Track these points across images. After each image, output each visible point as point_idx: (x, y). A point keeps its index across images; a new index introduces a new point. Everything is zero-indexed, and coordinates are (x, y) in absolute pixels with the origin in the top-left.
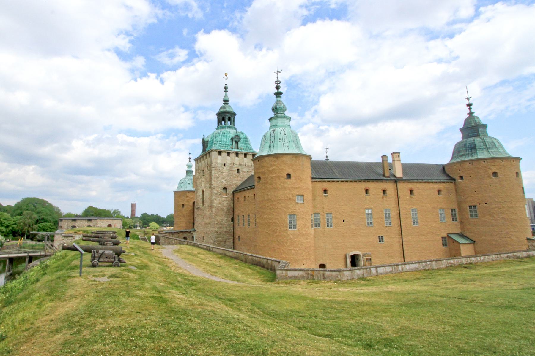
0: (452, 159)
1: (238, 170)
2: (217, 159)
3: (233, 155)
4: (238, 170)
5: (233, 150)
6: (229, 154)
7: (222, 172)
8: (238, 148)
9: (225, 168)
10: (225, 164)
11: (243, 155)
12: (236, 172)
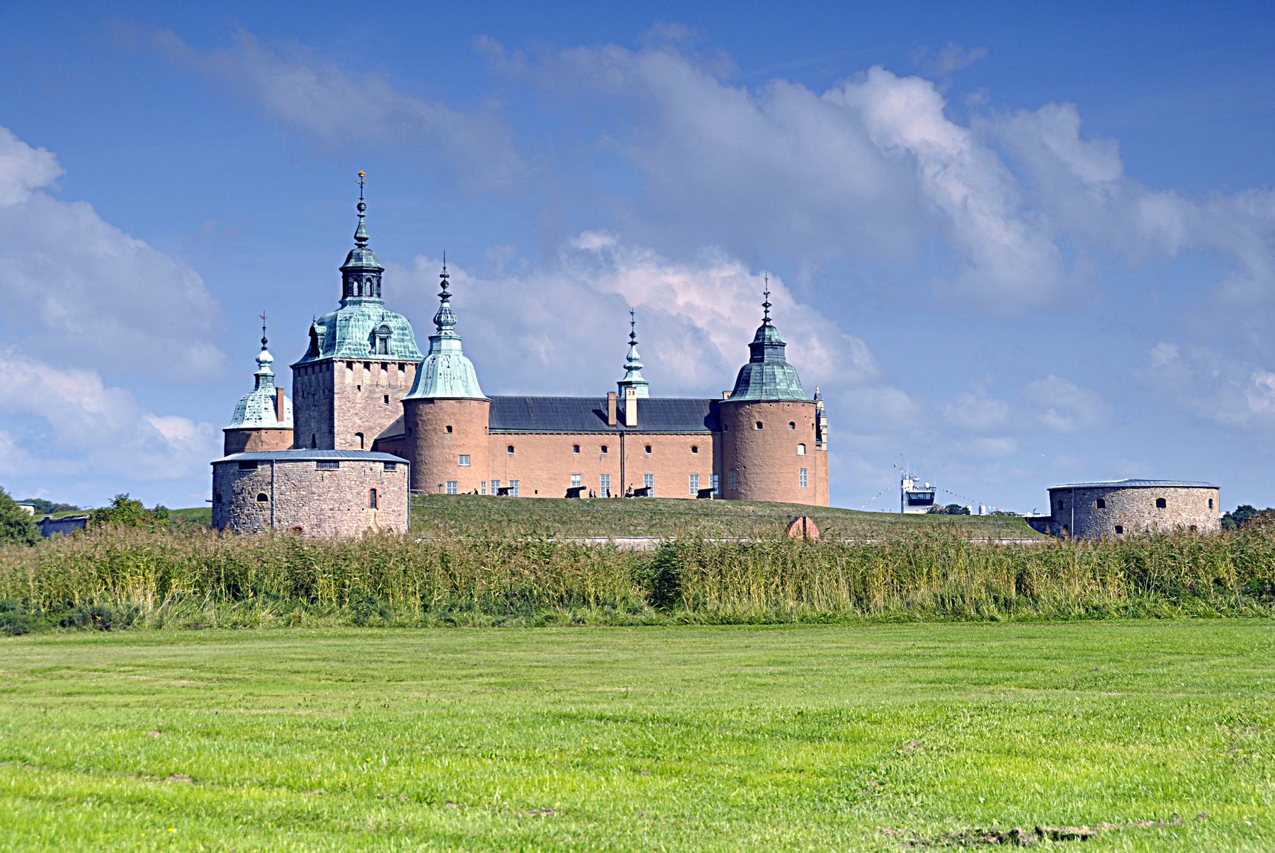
0: (734, 393)
1: (386, 398)
2: (343, 375)
4: (386, 398)
6: (367, 365)
7: (354, 403)
8: (386, 353)
9: (359, 394)
12: (383, 400)
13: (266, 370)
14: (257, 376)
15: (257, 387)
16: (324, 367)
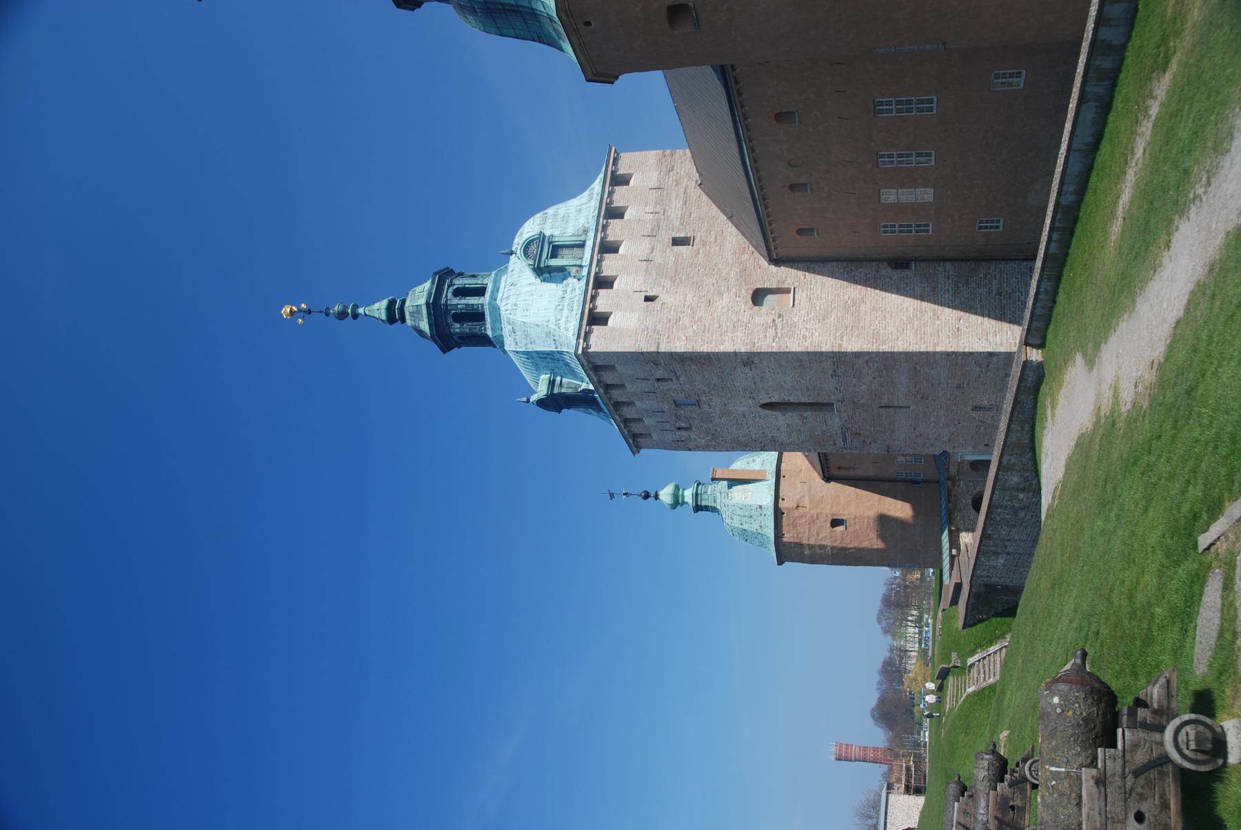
1: (676, 242)
3: (610, 265)
4: (676, 242)
5: (586, 262)
6: (603, 283)
8: (582, 245)
9: (663, 297)
10: (647, 299)
11: (614, 224)
13: (688, 495)
14: (698, 508)
15: (714, 510)
16: (609, 378)
